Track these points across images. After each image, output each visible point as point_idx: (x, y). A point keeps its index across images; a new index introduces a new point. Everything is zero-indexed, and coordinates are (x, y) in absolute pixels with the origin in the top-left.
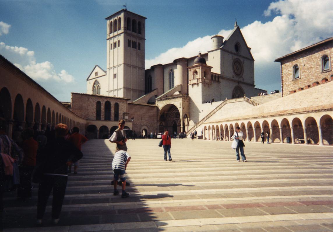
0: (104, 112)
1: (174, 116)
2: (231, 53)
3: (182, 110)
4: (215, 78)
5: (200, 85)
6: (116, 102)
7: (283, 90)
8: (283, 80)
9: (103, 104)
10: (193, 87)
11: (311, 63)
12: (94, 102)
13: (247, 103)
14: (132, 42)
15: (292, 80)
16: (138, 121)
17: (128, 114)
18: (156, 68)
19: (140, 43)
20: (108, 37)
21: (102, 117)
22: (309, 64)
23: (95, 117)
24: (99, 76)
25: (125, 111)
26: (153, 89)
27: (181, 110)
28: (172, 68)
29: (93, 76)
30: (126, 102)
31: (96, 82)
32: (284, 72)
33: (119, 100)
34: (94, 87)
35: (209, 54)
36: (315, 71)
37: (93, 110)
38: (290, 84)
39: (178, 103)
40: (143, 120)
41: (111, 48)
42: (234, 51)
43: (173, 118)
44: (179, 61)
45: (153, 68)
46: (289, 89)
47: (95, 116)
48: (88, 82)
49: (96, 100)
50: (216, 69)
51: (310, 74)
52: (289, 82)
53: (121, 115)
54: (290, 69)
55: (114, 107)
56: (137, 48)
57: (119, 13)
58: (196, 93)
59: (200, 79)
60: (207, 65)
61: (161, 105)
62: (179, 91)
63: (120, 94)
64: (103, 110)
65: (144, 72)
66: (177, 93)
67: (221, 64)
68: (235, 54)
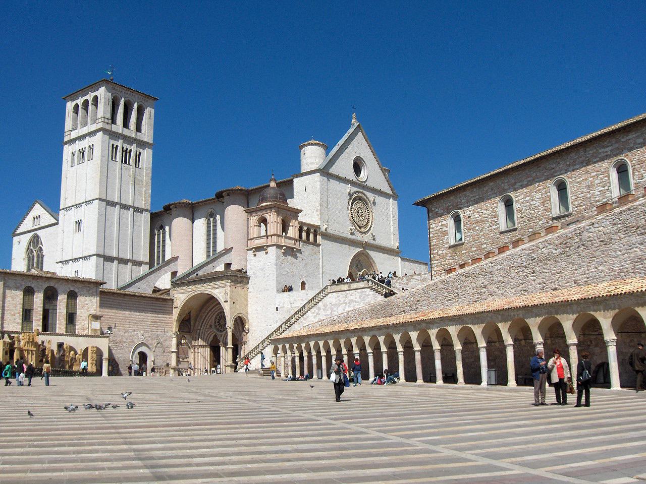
0: (42, 313)
1: (213, 322)
2: (345, 181)
3: (231, 308)
4: (310, 233)
5: (272, 250)
6: (72, 289)
7: (433, 266)
8: (432, 244)
10: (255, 255)
11: (482, 211)
13: (372, 293)
14: (119, 149)
15: (450, 247)
16: (126, 334)
17: (101, 317)
18: (175, 209)
19: (140, 153)
20: (66, 139)
22: (479, 212)
23: (18, 323)
24: (42, 225)
25: (93, 312)
26: (167, 258)
27: (226, 308)
28: (212, 210)
29: (27, 224)
30: (95, 288)
31: (35, 240)
32: (432, 228)
33: (79, 285)
34: (29, 251)
35: (294, 179)
36: (491, 228)
37: (15, 307)
38: (446, 254)
39: (220, 292)
40: (138, 332)
41: (73, 162)
42: (351, 175)
43: (211, 326)
44: (228, 195)
45: (167, 208)
46: (444, 265)
47: (20, 321)
48: (16, 239)
50: (309, 217)
51: (482, 233)
52: (443, 251)
53: (83, 320)
54: (444, 222)
55: (66, 300)
56: (132, 162)
57: (94, 87)
58: (263, 268)
59: (271, 236)
60: (289, 206)
61: (181, 297)
62: (228, 262)
63: (88, 271)
64: (40, 307)
65: (145, 218)
66: (220, 268)
67: (321, 205)
68: (353, 184)
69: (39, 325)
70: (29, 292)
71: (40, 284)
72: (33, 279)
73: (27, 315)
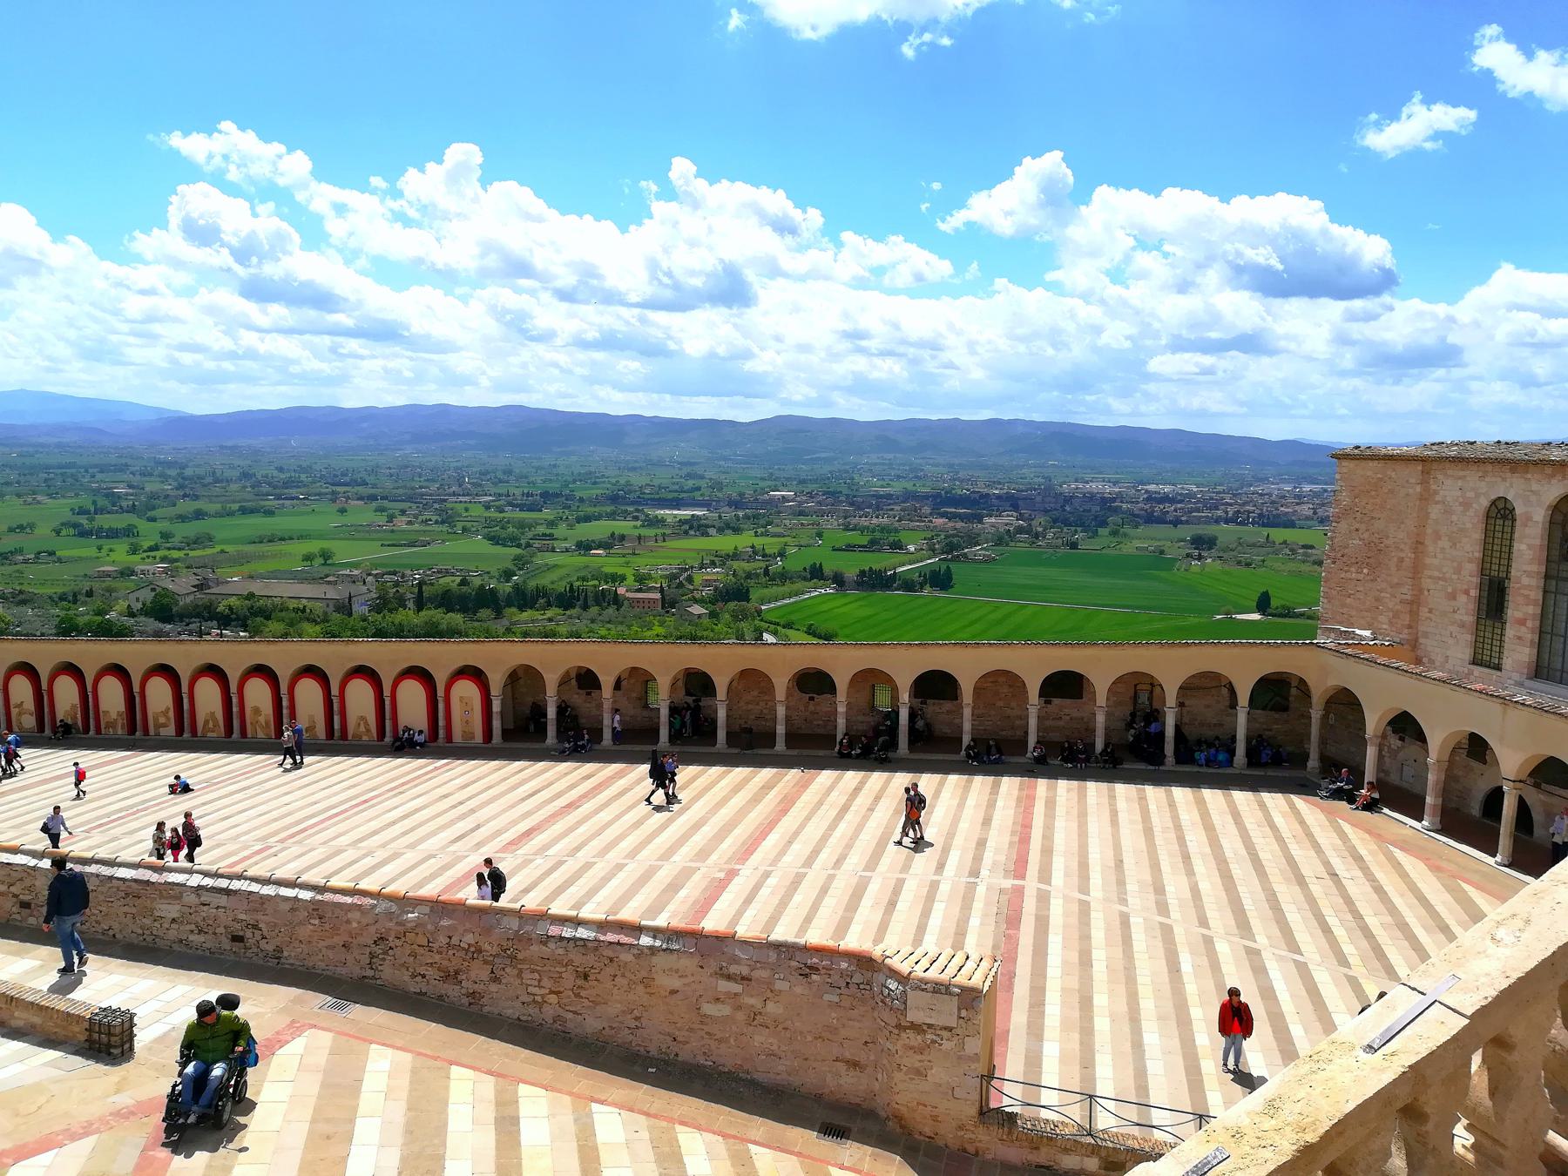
9: (1529, 518)
12: (1466, 505)
21: (1510, 632)
23: (1462, 625)
37: (1458, 570)
47: (1470, 619)
49: (1483, 486)
69: (1519, 638)
70: (1501, 514)
71: (1535, 487)
72: (1513, 471)
73: (1493, 599)
